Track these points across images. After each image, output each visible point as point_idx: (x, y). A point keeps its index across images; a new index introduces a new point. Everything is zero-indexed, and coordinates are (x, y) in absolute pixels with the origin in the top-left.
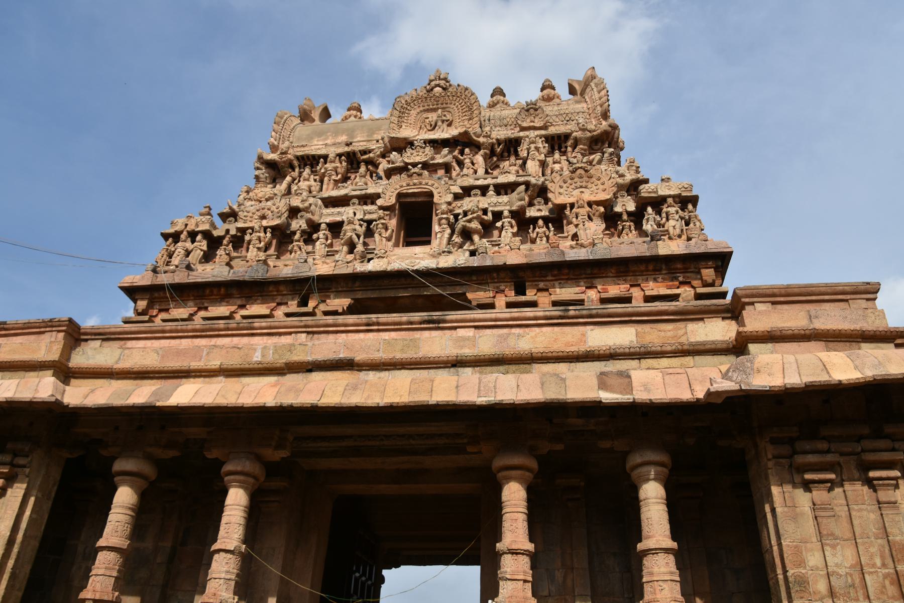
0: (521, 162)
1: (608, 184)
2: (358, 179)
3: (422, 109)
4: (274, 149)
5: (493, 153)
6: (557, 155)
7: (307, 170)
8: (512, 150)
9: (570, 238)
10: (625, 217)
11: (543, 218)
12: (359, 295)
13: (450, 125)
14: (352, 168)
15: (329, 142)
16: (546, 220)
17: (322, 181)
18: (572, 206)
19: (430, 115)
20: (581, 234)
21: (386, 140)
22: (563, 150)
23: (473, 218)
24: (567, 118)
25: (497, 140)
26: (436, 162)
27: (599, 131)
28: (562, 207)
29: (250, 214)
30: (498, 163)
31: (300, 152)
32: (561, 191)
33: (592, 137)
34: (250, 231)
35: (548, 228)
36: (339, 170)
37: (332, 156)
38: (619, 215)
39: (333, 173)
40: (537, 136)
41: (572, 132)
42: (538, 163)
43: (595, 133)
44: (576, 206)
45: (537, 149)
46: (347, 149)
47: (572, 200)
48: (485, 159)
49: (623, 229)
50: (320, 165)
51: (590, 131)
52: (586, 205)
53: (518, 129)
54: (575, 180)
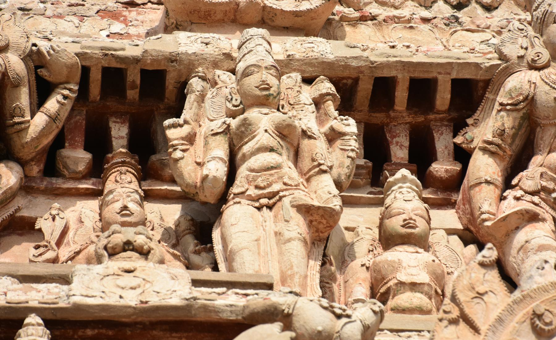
0: (172, 213)
6: (405, 196)
8: (119, 133)
22: (441, 168)
25: (35, 59)
30: (26, 207)
40: (282, 67)
42: (297, 227)
45: (290, 138)
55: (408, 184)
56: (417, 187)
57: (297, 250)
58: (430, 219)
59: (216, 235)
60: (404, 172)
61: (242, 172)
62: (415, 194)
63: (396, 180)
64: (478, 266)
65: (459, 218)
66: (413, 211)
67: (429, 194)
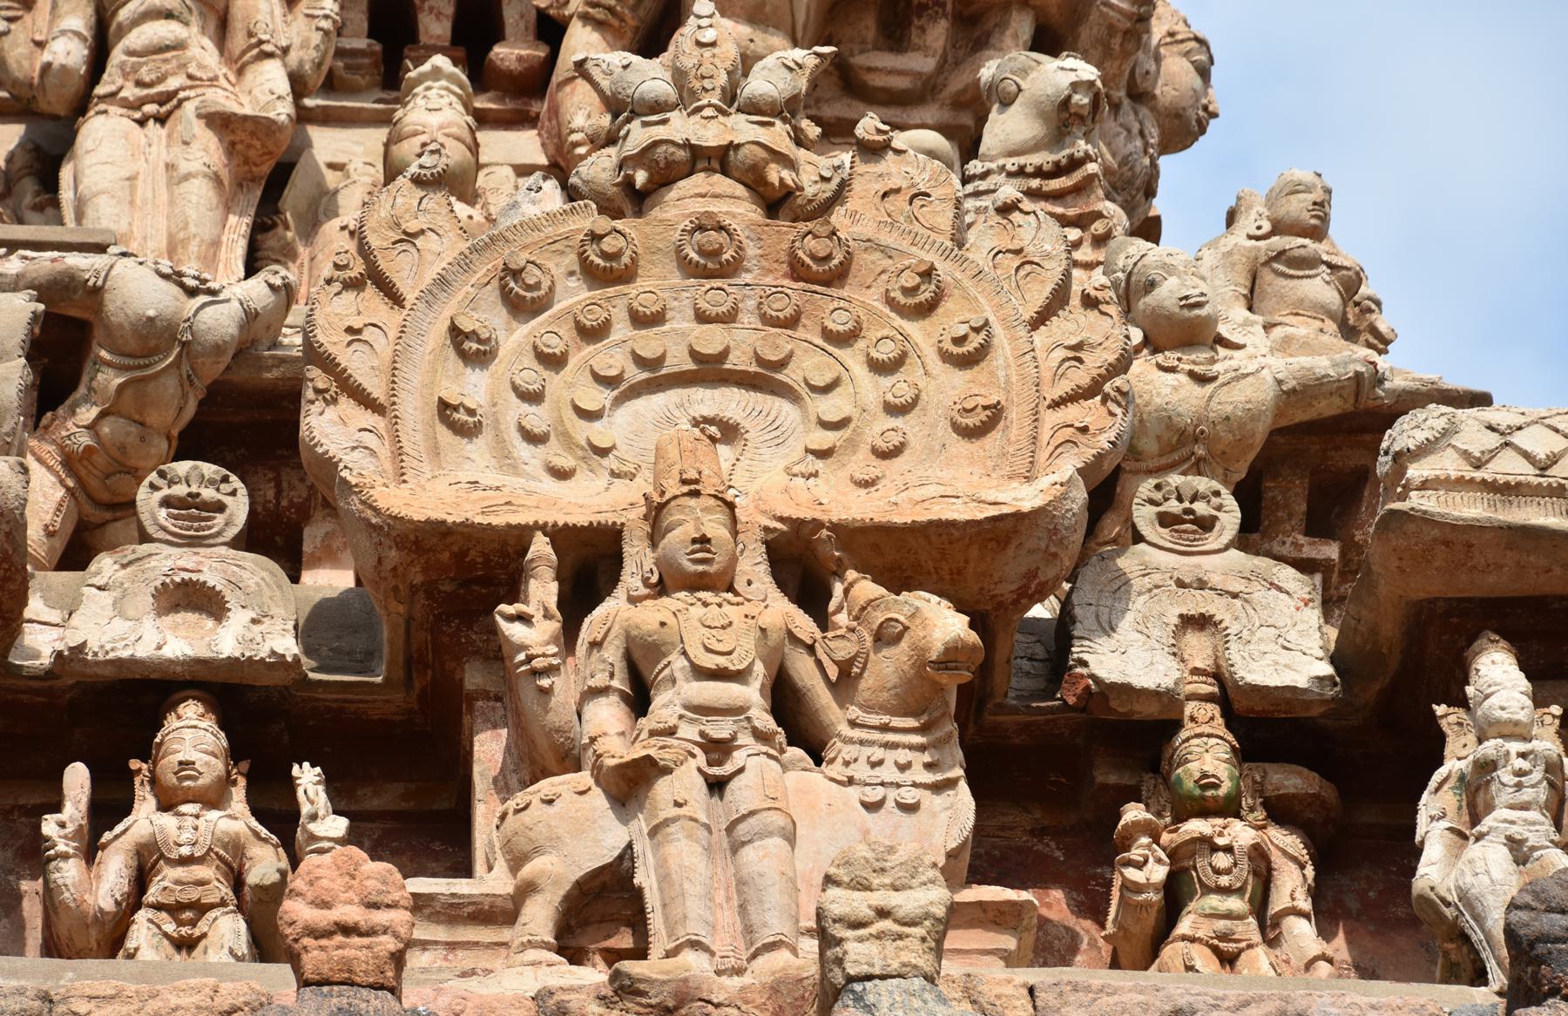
1: (1022, 365)
6: (436, 103)
9: (539, 917)
10: (1207, 755)
11: (232, 693)
16: (266, 721)
18: (590, 564)
20: (682, 877)
22: (509, 54)
28: (462, 575)
32: (473, 388)
35: (279, 816)
38: (1138, 735)
42: (205, 151)
44: (638, 561)
47: (587, 500)
49: (1175, 894)
52: (754, 569)
54: (645, 290)
55: (443, 83)
56: (461, 87)
57: (199, 197)
58: (477, 145)
59: (66, 174)
60: (440, 60)
61: (117, 56)
62: (454, 99)
63: (421, 74)
64: (409, 184)
65: (543, 145)
66: (441, 127)
67: (489, 100)
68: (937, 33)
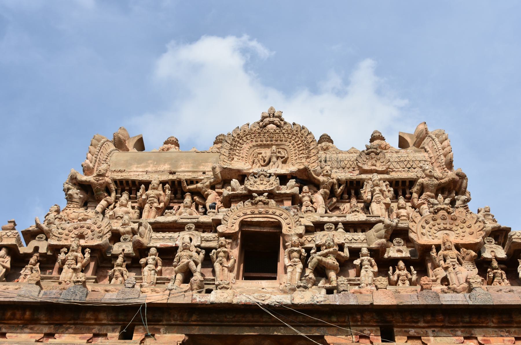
0: (362, 205)
1: (475, 228)
2: (182, 209)
3: (254, 143)
4: (87, 170)
5: (332, 193)
7: (125, 196)
8: (353, 192)
9: (439, 281)
10: (495, 264)
11: (404, 259)
12: (196, 331)
13: (284, 162)
14: (175, 198)
15: (149, 169)
16: (408, 262)
17: (141, 209)
18: (438, 248)
19: (263, 151)
20: (452, 277)
21: (218, 170)
22: (407, 196)
23: (330, 253)
24: (409, 166)
25: (338, 180)
26: (283, 192)
27: (447, 179)
28: (427, 248)
29: (66, 232)
31: (118, 176)
32: (424, 231)
33: (439, 184)
34: (65, 250)
35: (409, 271)
36: (162, 198)
37: (155, 182)
38: (488, 262)
39: (156, 200)
40: (380, 180)
41: (418, 178)
42: (384, 206)
43: (443, 181)
44: (443, 247)
45: (382, 192)
46: (171, 177)
47: (436, 242)
48: (324, 199)
49: (494, 277)
50: (141, 191)
51: (437, 179)
52: (453, 248)
53: (358, 172)
54: (439, 221)
57: (384, 210)
59: (370, 208)
61: (374, 198)
68: (447, 193)
